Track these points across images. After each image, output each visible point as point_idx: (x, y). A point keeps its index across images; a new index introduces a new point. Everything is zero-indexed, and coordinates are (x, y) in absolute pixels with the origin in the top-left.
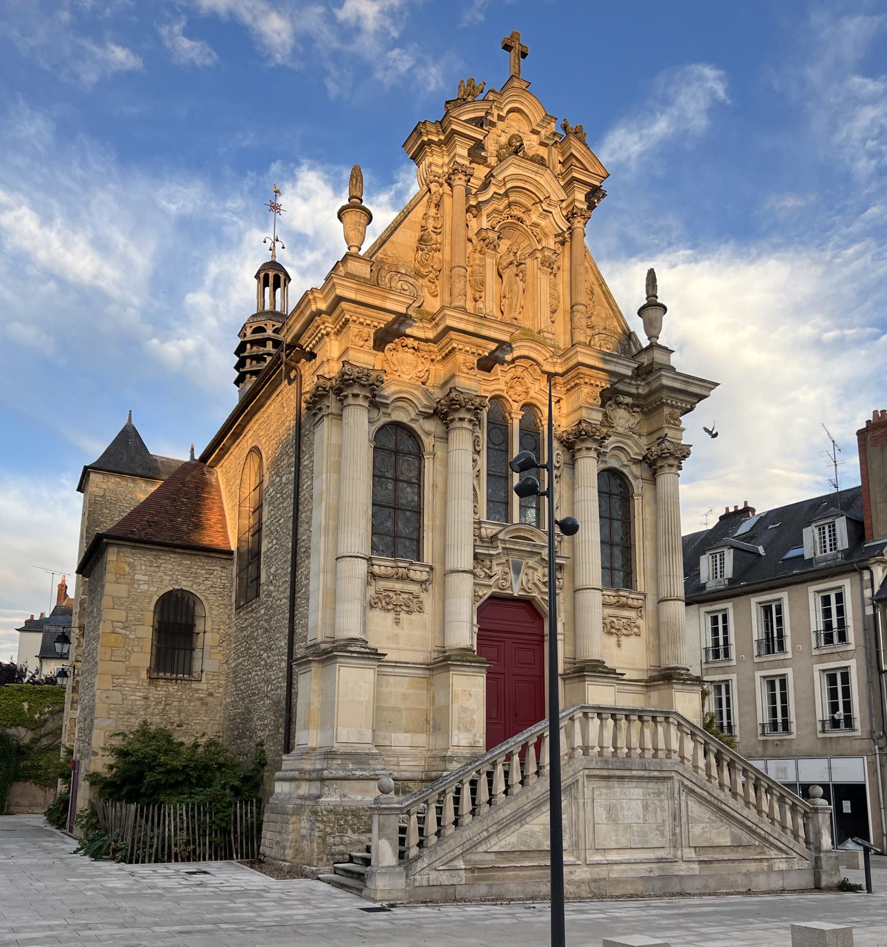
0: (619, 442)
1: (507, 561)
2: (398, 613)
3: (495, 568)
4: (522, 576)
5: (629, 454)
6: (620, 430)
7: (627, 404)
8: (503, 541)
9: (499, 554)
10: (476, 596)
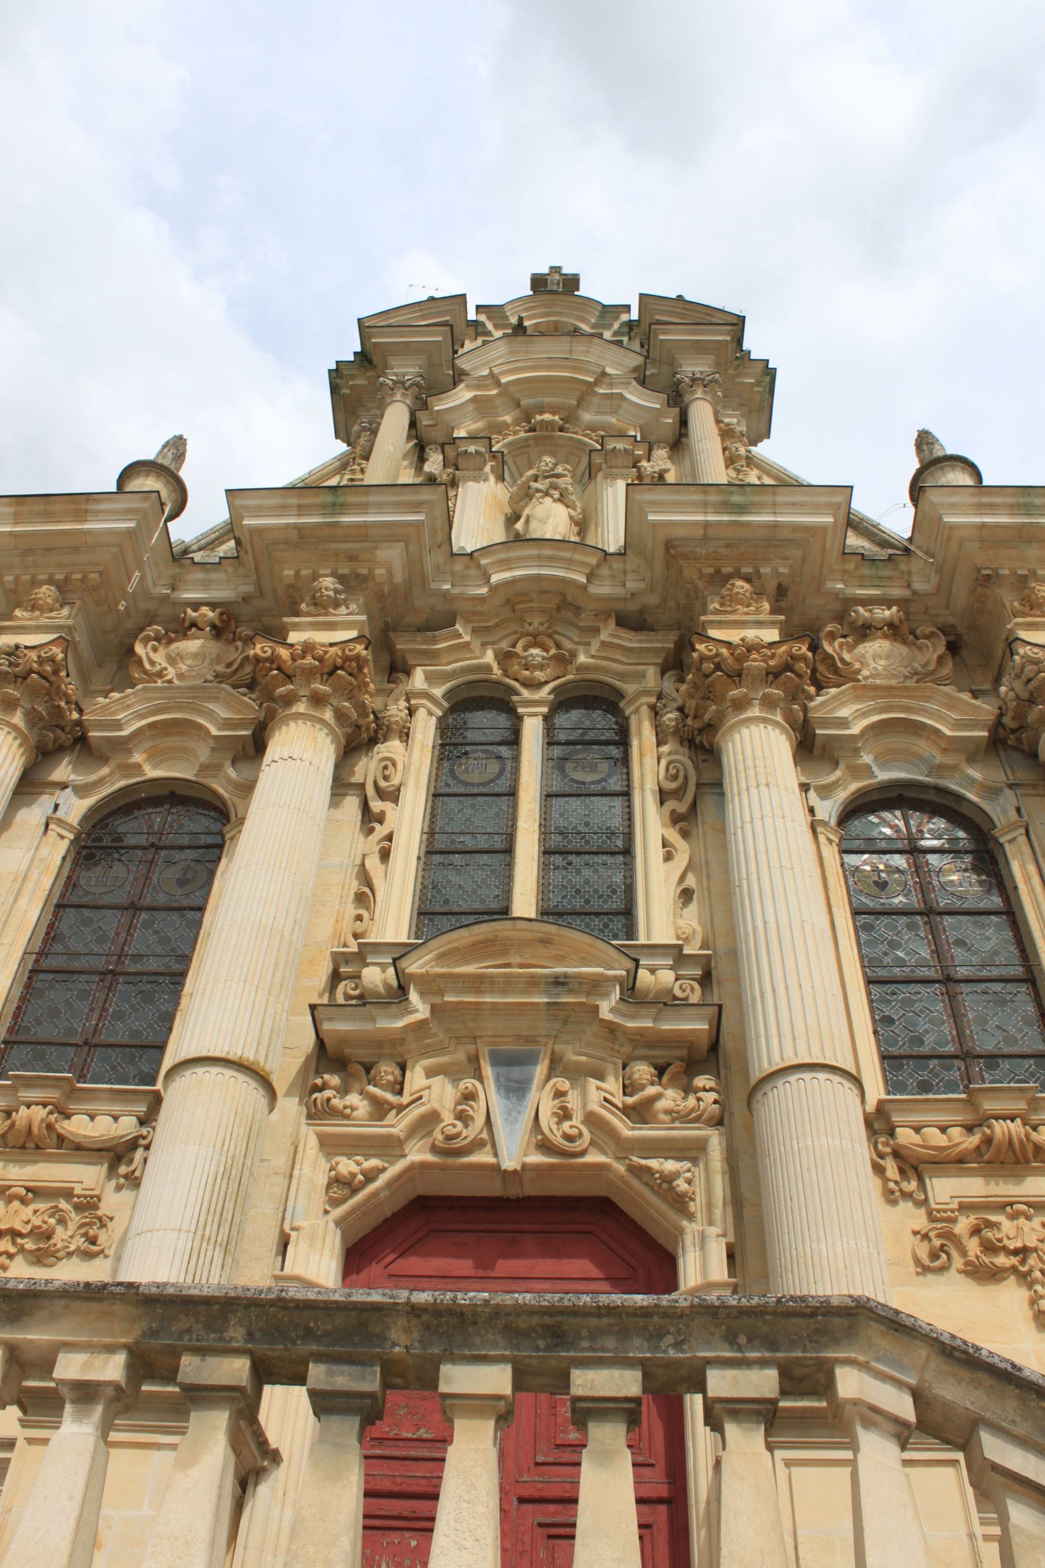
0: (889, 709)
3: (416, 1078)
4: (542, 1099)
5: (937, 732)
7: (891, 625)
8: (429, 985)
10: (341, 1186)
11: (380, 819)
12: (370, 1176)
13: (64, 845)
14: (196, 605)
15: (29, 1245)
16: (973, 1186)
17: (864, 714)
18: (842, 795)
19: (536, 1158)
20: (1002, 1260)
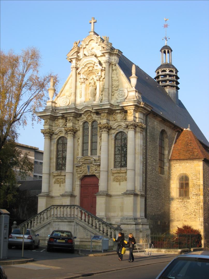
1: (86, 166)
2: (60, 184)
6: (119, 120)
8: (82, 162)
9: (82, 165)
11: (78, 141)
12: (80, 176)
13: (56, 145)
14: (59, 116)
15: (62, 182)
16: (117, 175)
17: (116, 125)
18: (115, 134)
19: (90, 174)
20: (118, 180)
